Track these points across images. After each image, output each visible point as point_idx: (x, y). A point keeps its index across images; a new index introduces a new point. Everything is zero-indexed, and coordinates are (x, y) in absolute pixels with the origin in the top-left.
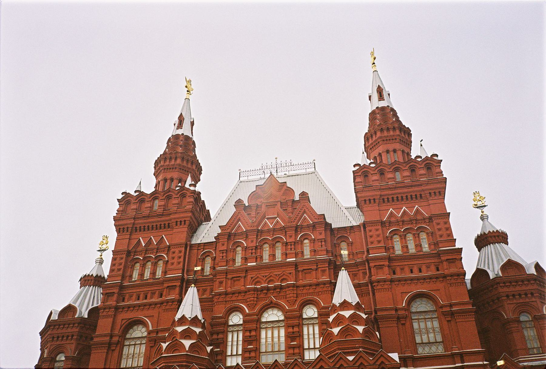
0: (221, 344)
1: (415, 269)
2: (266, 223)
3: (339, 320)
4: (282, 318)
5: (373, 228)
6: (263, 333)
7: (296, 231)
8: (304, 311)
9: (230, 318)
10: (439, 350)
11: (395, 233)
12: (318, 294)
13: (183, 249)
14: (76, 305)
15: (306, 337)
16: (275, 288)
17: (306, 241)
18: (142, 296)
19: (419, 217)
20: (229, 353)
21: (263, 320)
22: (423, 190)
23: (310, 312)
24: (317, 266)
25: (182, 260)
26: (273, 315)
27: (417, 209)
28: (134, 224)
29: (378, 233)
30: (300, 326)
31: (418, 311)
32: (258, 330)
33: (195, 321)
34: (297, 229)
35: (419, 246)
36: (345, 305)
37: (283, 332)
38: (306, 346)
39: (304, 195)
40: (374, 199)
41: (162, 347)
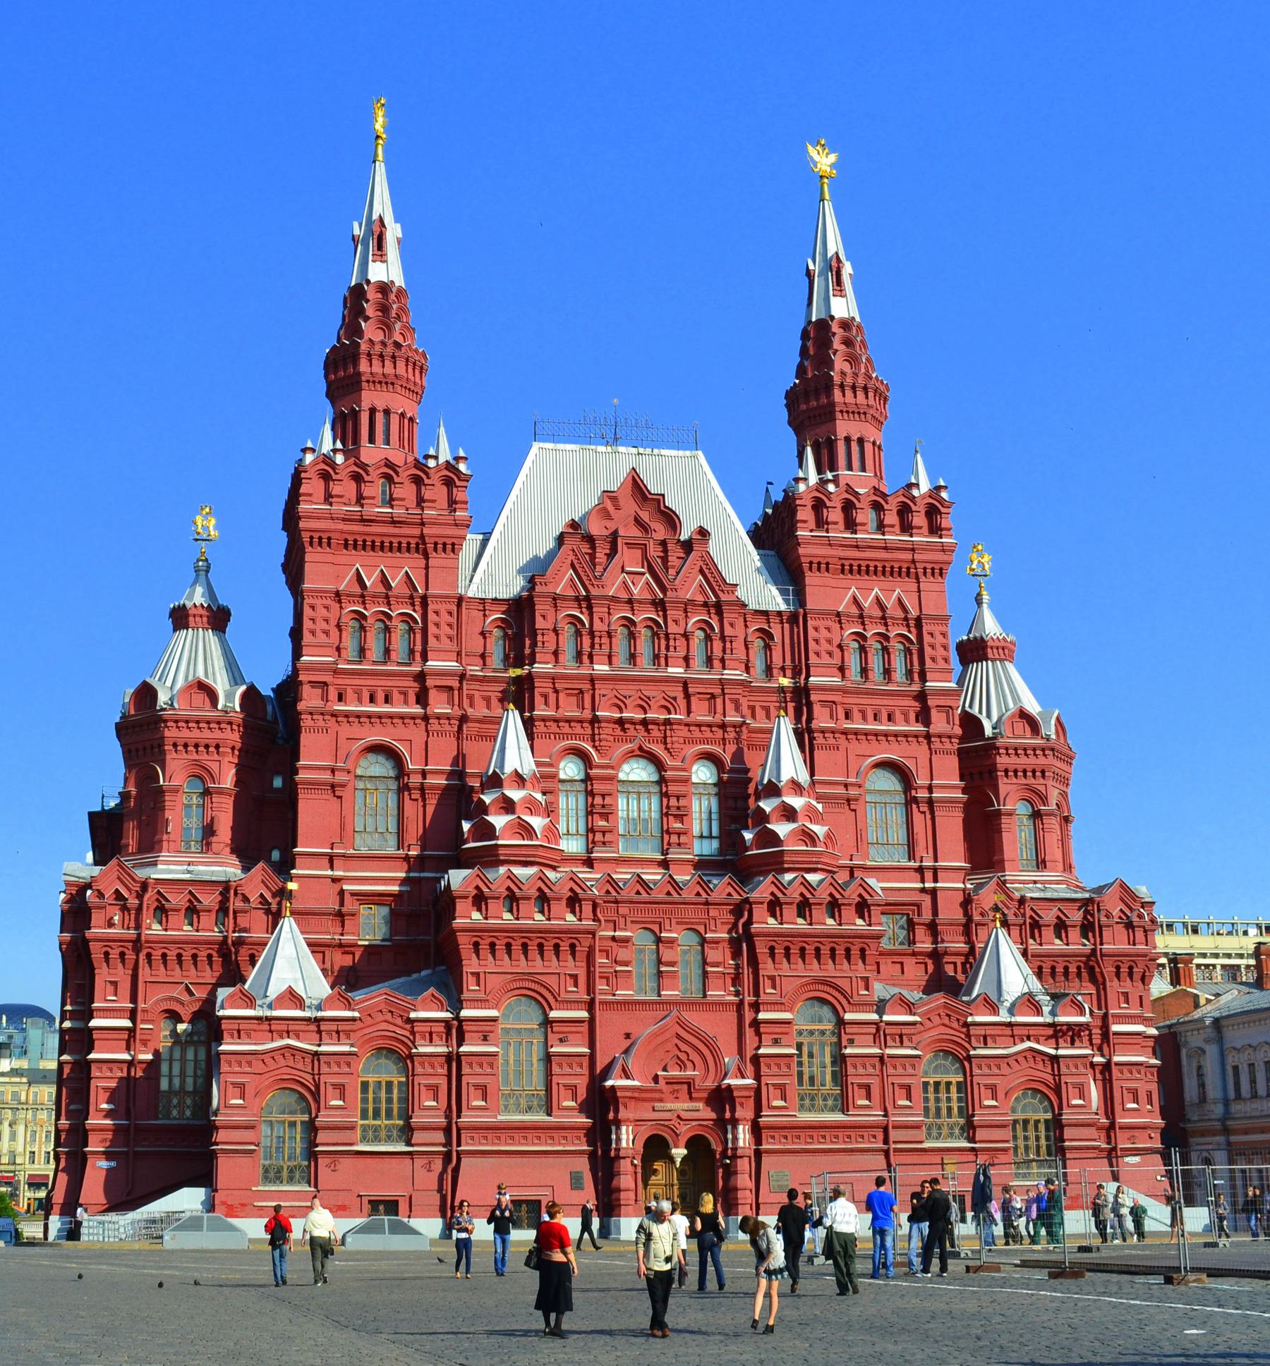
0: (550, 811)
5: (821, 624)
6: (622, 802)
7: (686, 611)
16: (645, 723)
18: (380, 696)
22: (913, 561)
24: (723, 690)
37: (655, 801)
39: (703, 533)
40: (827, 564)
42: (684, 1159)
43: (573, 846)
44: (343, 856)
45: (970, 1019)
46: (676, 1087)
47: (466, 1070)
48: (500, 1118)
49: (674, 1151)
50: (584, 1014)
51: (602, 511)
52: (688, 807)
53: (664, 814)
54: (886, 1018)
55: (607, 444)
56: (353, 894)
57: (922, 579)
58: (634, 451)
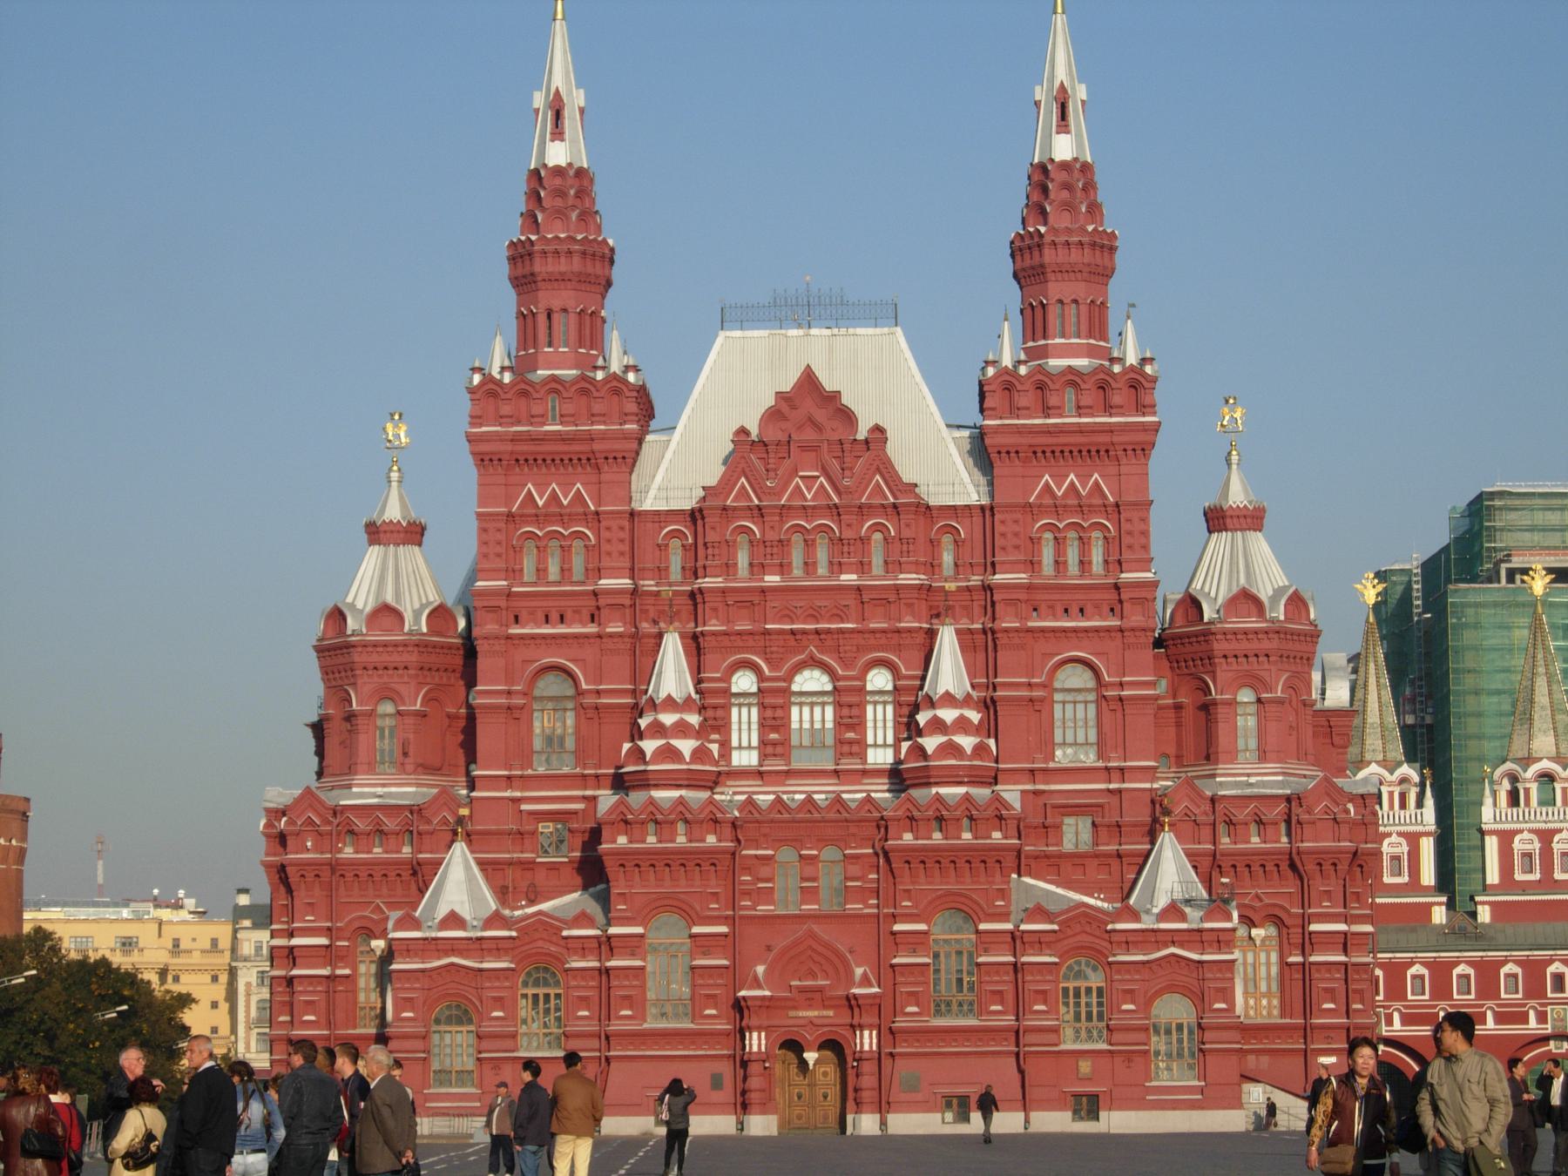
1: (1074, 610)
2: (798, 486)
3: (938, 726)
4: (829, 687)
6: (795, 711)
8: (870, 676)
9: (734, 679)
10: (1089, 758)
11: (1050, 527)
12: (898, 649)
13: (626, 524)
14: (389, 598)
15: (870, 724)
16: (817, 632)
17: (878, 536)
18: (554, 616)
19: (1097, 501)
20: (735, 743)
21: (795, 688)
23: (879, 680)
25: (626, 548)
26: (811, 681)
27: (1096, 482)
28: (512, 453)
29: (1017, 528)
30: (862, 706)
31: (1067, 686)
32: (786, 708)
33: (687, 705)
34: (863, 511)
35: (1084, 564)
36: (949, 699)
37: (829, 711)
38: (870, 740)
39: (878, 429)
41: (642, 752)
42: (817, 1062)
43: (745, 758)
44: (521, 777)
45: (1109, 927)
46: (810, 995)
47: (614, 983)
48: (645, 1026)
49: (805, 1055)
50: (723, 929)
51: (772, 416)
52: (863, 715)
53: (838, 723)
54: (1023, 927)
55: (800, 326)
56: (531, 813)
57: (1124, 461)
58: (828, 332)
